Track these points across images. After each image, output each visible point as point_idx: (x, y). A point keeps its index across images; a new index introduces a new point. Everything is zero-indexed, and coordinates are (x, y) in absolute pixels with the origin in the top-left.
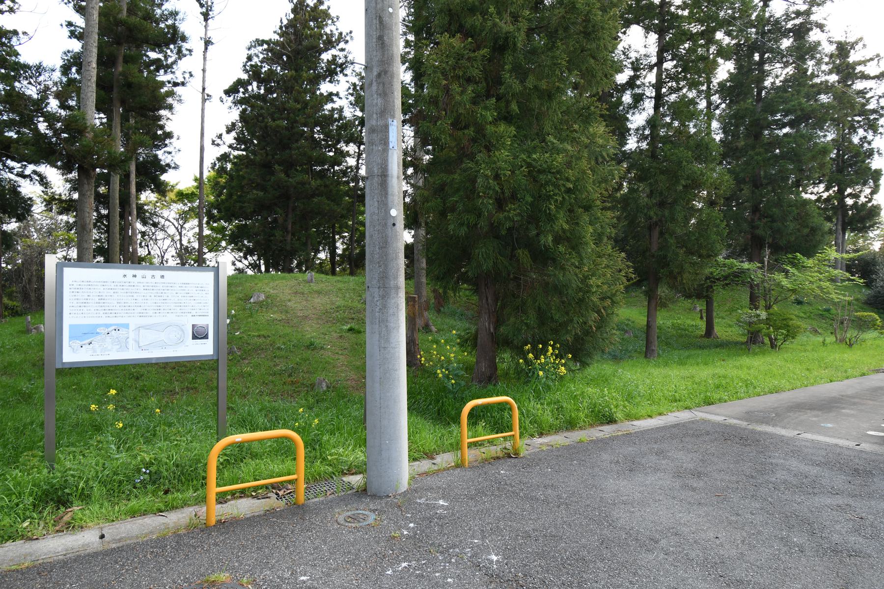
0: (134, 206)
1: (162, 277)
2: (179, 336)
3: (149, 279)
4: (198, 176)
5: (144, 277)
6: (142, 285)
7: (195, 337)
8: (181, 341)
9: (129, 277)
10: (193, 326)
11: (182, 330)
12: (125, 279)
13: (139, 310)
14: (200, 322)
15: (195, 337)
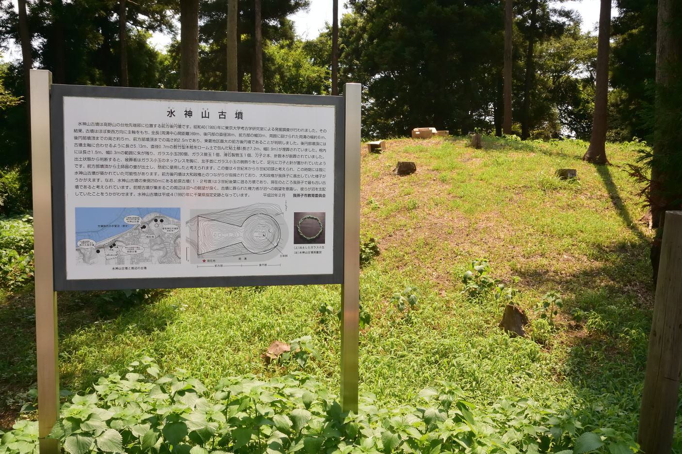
0: (260, 56)
1: (239, 115)
2: (269, 236)
3: (214, 120)
4: (331, 24)
5: (205, 116)
6: (201, 131)
7: (299, 239)
8: (273, 246)
9: (180, 118)
10: (297, 216)
11: (277, 224)
12: (172, 120)
13: (196, 181)
14: (310, 207)
15: (299, 239)
